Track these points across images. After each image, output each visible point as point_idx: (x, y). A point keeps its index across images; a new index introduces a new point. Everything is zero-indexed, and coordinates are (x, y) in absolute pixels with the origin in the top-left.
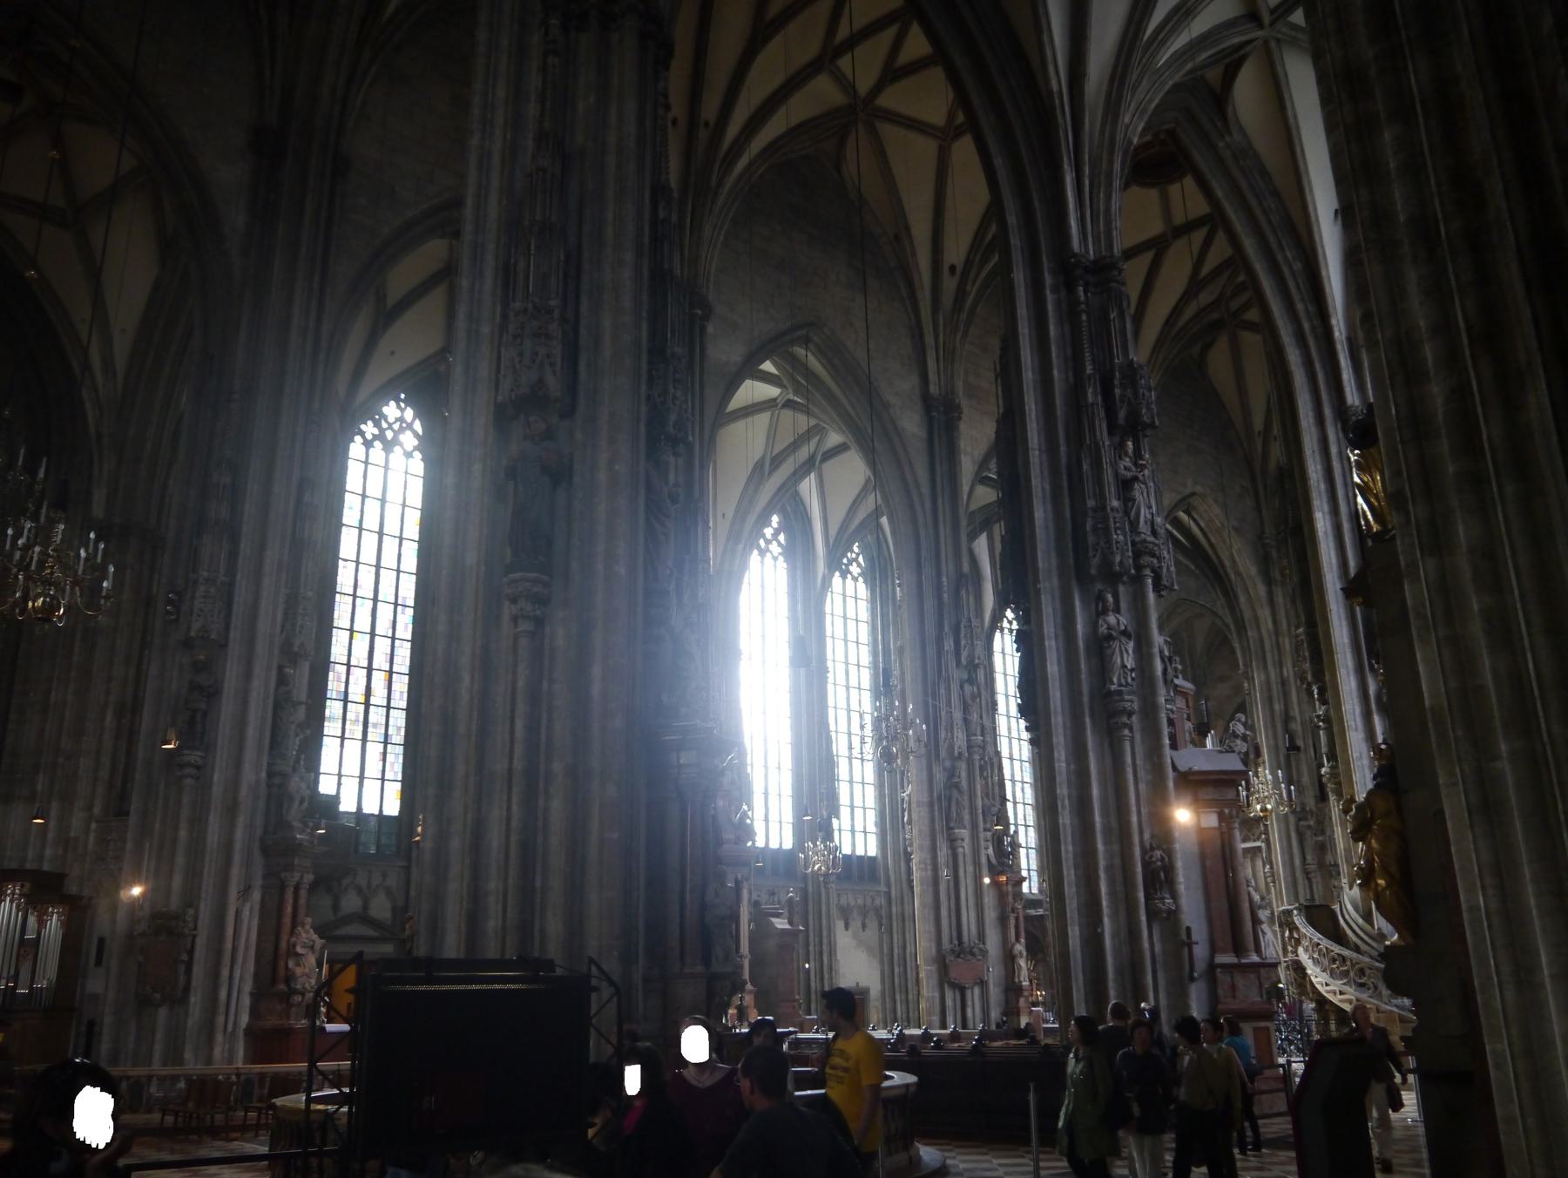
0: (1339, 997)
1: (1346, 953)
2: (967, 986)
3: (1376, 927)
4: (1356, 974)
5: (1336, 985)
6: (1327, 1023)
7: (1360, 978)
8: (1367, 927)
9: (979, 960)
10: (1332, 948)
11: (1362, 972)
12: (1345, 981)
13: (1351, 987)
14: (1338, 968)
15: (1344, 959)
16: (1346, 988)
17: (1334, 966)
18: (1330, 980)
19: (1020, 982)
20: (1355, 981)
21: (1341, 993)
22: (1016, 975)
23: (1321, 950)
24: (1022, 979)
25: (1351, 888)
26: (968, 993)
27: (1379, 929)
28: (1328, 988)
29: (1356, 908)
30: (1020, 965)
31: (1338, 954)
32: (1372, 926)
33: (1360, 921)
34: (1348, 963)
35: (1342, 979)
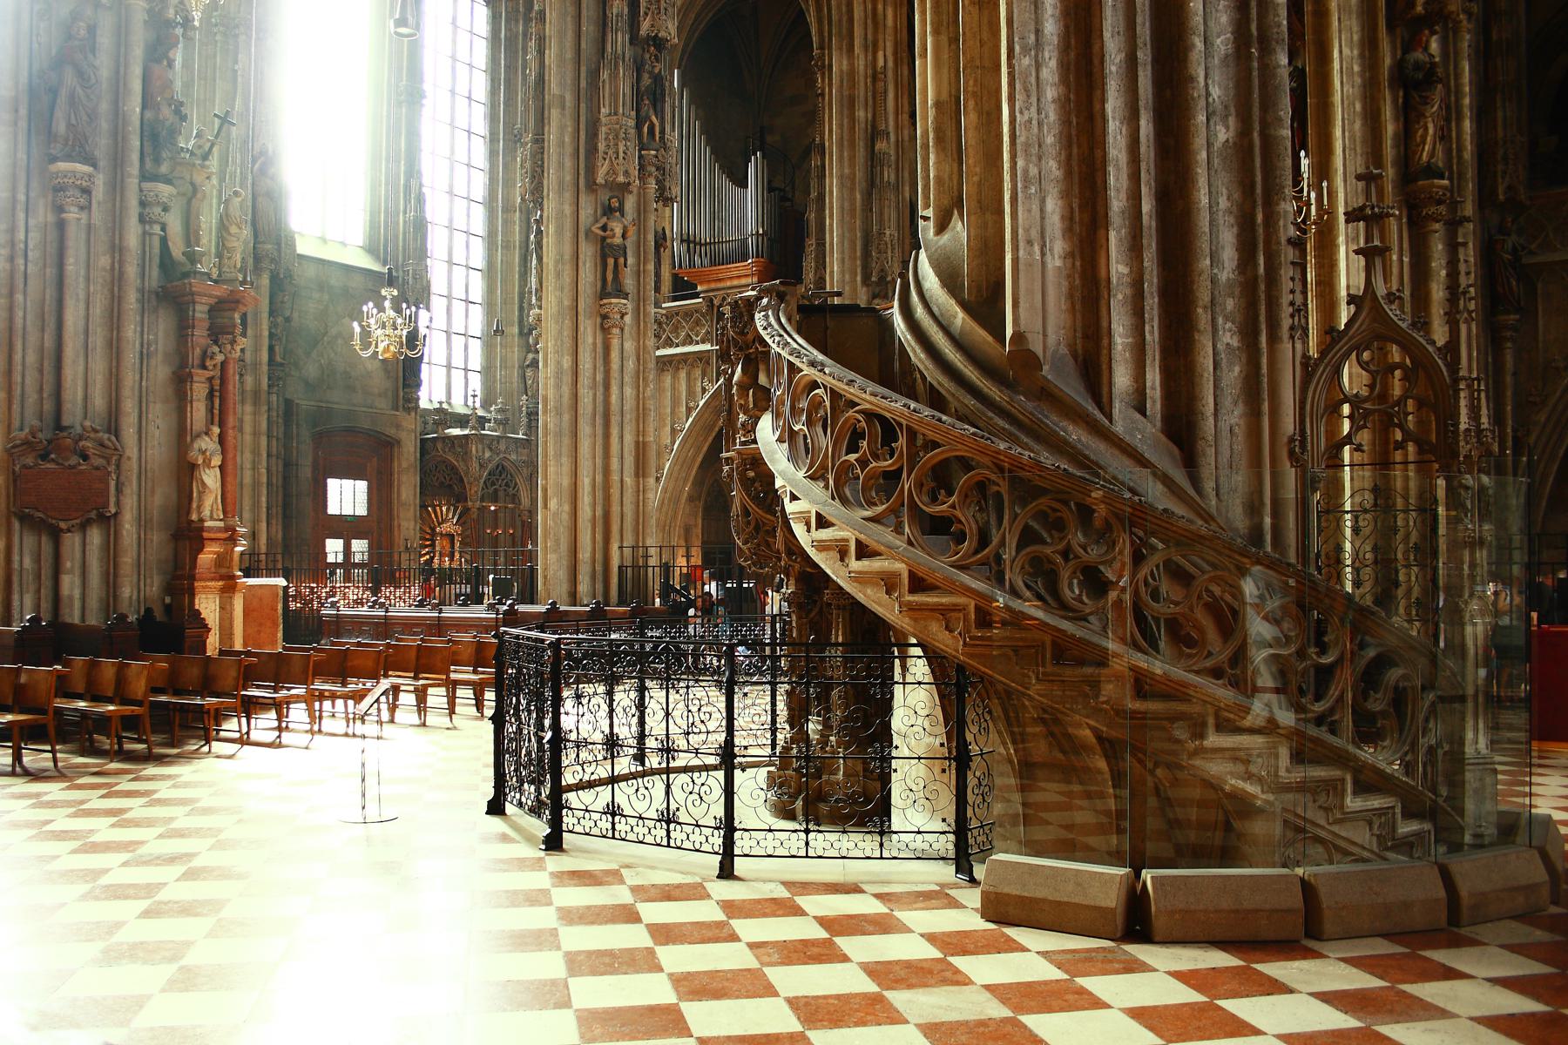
0: (855, 565)
1: (896, 406)
2: (63, 525)
3: (1009, 332)
4: (920, 485)
5: (852, 525)
6: (823, 642)
7: (934, 500)
8: (981, 335)
9: (97, 468)
10: (852, 392)
11: (941, 478)
12: (880, 509)
13: (898, 530)
14: (863, 463)
15: (888, 429)
16: (882, 536)
17: (853, 457)
18: (833, 510)
19: (202, 520)
20: (913, 506)
21: (863, 552)
22: (194, 505)
23: (816, 405)
24: (206, 513)
25: (942, 227)
26: (71, 542)
27: (1018, 336)
28: (825, 534)
29: (950, 280)
30: (203, 484)
31: (870, 415)
32: (998, 331)
33: (959, 317)
34: (902, 442)
35: (871, 504)
